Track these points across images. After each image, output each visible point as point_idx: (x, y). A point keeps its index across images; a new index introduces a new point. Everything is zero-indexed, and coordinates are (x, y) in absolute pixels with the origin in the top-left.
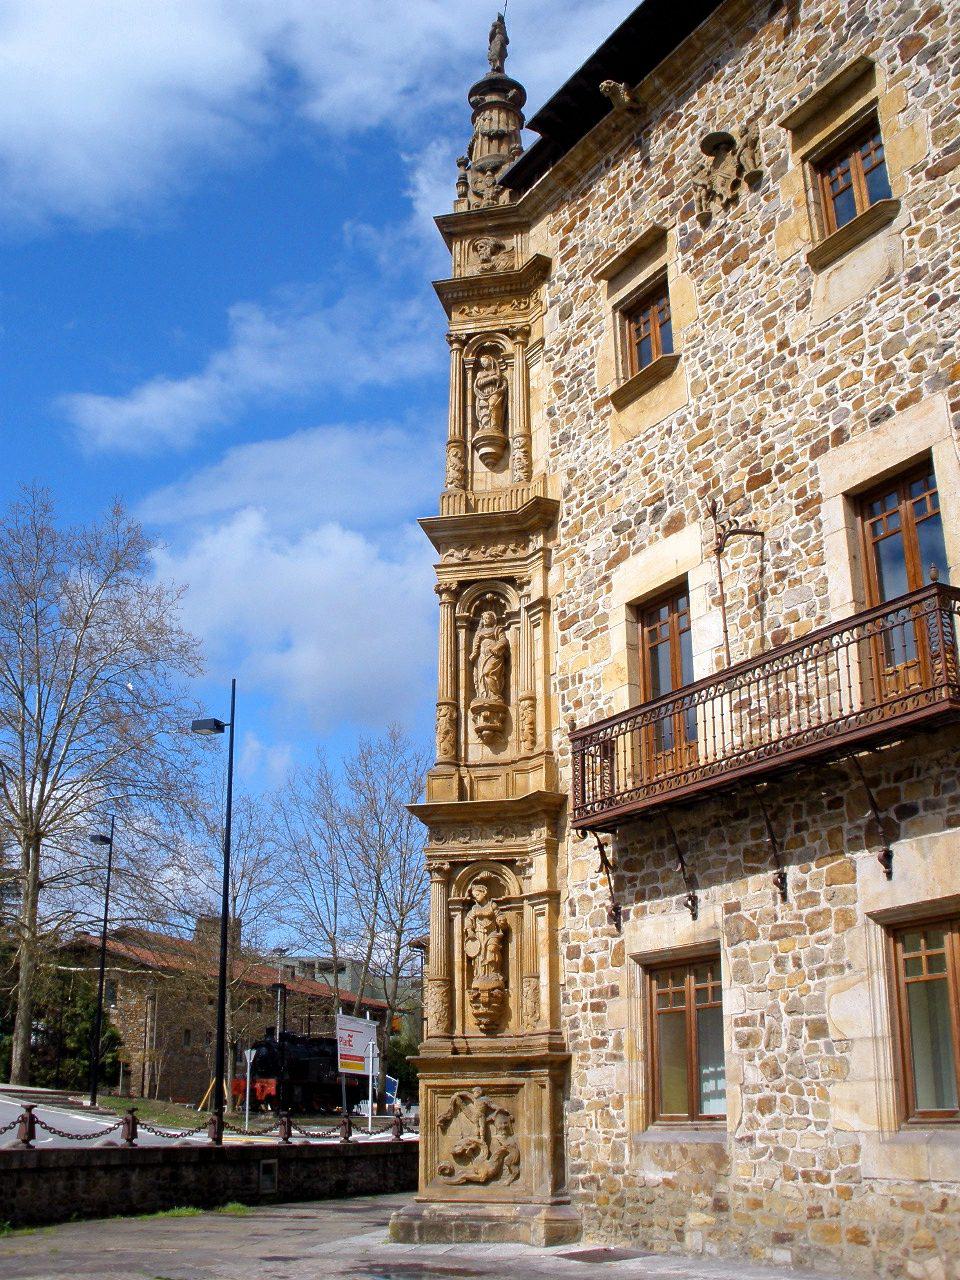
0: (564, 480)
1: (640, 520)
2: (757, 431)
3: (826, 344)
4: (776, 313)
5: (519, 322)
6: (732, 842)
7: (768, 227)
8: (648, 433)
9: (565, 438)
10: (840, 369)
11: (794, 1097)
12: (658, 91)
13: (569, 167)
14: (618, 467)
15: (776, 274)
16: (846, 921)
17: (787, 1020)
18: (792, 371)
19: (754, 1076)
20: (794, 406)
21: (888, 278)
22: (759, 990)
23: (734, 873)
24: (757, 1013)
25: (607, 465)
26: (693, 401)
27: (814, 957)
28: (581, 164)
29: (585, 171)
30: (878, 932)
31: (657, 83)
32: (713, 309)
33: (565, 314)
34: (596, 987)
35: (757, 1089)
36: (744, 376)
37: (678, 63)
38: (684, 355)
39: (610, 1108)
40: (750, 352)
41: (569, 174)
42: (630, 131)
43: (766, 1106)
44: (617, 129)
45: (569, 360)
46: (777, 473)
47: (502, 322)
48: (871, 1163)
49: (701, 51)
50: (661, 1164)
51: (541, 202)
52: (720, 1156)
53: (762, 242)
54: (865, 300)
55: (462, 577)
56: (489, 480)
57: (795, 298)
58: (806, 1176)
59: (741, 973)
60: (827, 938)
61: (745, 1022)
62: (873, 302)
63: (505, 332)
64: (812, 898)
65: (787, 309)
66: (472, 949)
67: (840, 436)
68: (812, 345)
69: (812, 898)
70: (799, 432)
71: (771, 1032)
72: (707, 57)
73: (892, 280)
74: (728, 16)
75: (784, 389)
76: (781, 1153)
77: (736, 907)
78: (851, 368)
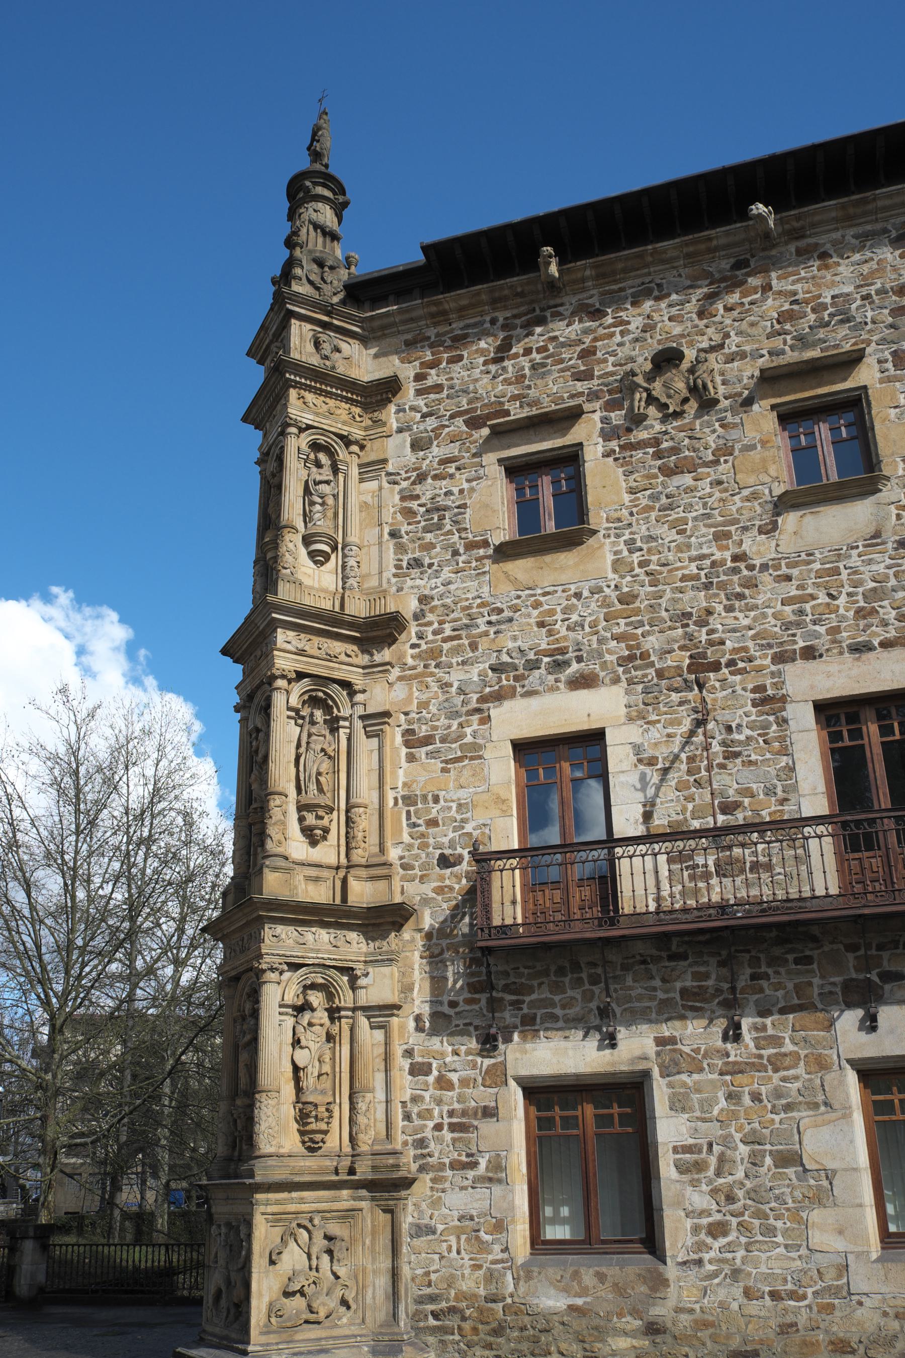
1: (533, 665)
2: (702, 623)
3: (795, 572)
4: (732, 528)
5: (357, 433)
6: (664, 980)
8: (547, 590)
9: (417, 563)
10: (813, 597)
11: (756, 1222)
12: (583, 280)
13: (447, 307)
14: (500, 611)
15: (732, 495)
16: (821, 1064)
17: (744, 1150)
18: (751, 584)
19: (699, 1199)
20: (752, 614)
21: (873, 537)
22: (704, 1120)
23: (668, 1011)
24: (704, 1142)
25: (482, 605)
26: (611, 575)
27: (778, 1094)
28: (462, 309)
29: (461, 318)
30: (852, 1077)
31: (588, 273)
32: (644, 502)
33: (417, 445)
34: (456, 1106)
35: (703, 1213)
36: (686, 572)
38: (603, 532)
39: (482, 1234)
40: (694, 553)
41: (444, 313)
42: (532, 302)
43: (718, 1230)
44: (521, 295)
45: (428, 490)
46: (728, 665)
47: (340, 426)
48: (861, 1279)
49: (647, 266)
50: (566, 1290)
51: (394, 324)
52: (659, 1283)
53: (716, 462)
54: (845, 548)
55: (300, 667)
56: (316, 578)
57: (758, 523)
58: (775, 1295)
59: (678, 1104)
60: (796, 1078)
61: (688, 1149)
62: (854, 553)
63: (341, 437)
64: (776, 1041)
65: (745, 529)
66: (302, 1058)
67: (810, 653)
68: (777, 567)
69: (776, 1041)
70: (754, 638)
71: (722, 1159)
72: (649, 274)
73: (879, 540)
74: (691, 249)
75: (740, 596)
76: (736, 1274)
77: (672, 1040)
78: (823, 599)
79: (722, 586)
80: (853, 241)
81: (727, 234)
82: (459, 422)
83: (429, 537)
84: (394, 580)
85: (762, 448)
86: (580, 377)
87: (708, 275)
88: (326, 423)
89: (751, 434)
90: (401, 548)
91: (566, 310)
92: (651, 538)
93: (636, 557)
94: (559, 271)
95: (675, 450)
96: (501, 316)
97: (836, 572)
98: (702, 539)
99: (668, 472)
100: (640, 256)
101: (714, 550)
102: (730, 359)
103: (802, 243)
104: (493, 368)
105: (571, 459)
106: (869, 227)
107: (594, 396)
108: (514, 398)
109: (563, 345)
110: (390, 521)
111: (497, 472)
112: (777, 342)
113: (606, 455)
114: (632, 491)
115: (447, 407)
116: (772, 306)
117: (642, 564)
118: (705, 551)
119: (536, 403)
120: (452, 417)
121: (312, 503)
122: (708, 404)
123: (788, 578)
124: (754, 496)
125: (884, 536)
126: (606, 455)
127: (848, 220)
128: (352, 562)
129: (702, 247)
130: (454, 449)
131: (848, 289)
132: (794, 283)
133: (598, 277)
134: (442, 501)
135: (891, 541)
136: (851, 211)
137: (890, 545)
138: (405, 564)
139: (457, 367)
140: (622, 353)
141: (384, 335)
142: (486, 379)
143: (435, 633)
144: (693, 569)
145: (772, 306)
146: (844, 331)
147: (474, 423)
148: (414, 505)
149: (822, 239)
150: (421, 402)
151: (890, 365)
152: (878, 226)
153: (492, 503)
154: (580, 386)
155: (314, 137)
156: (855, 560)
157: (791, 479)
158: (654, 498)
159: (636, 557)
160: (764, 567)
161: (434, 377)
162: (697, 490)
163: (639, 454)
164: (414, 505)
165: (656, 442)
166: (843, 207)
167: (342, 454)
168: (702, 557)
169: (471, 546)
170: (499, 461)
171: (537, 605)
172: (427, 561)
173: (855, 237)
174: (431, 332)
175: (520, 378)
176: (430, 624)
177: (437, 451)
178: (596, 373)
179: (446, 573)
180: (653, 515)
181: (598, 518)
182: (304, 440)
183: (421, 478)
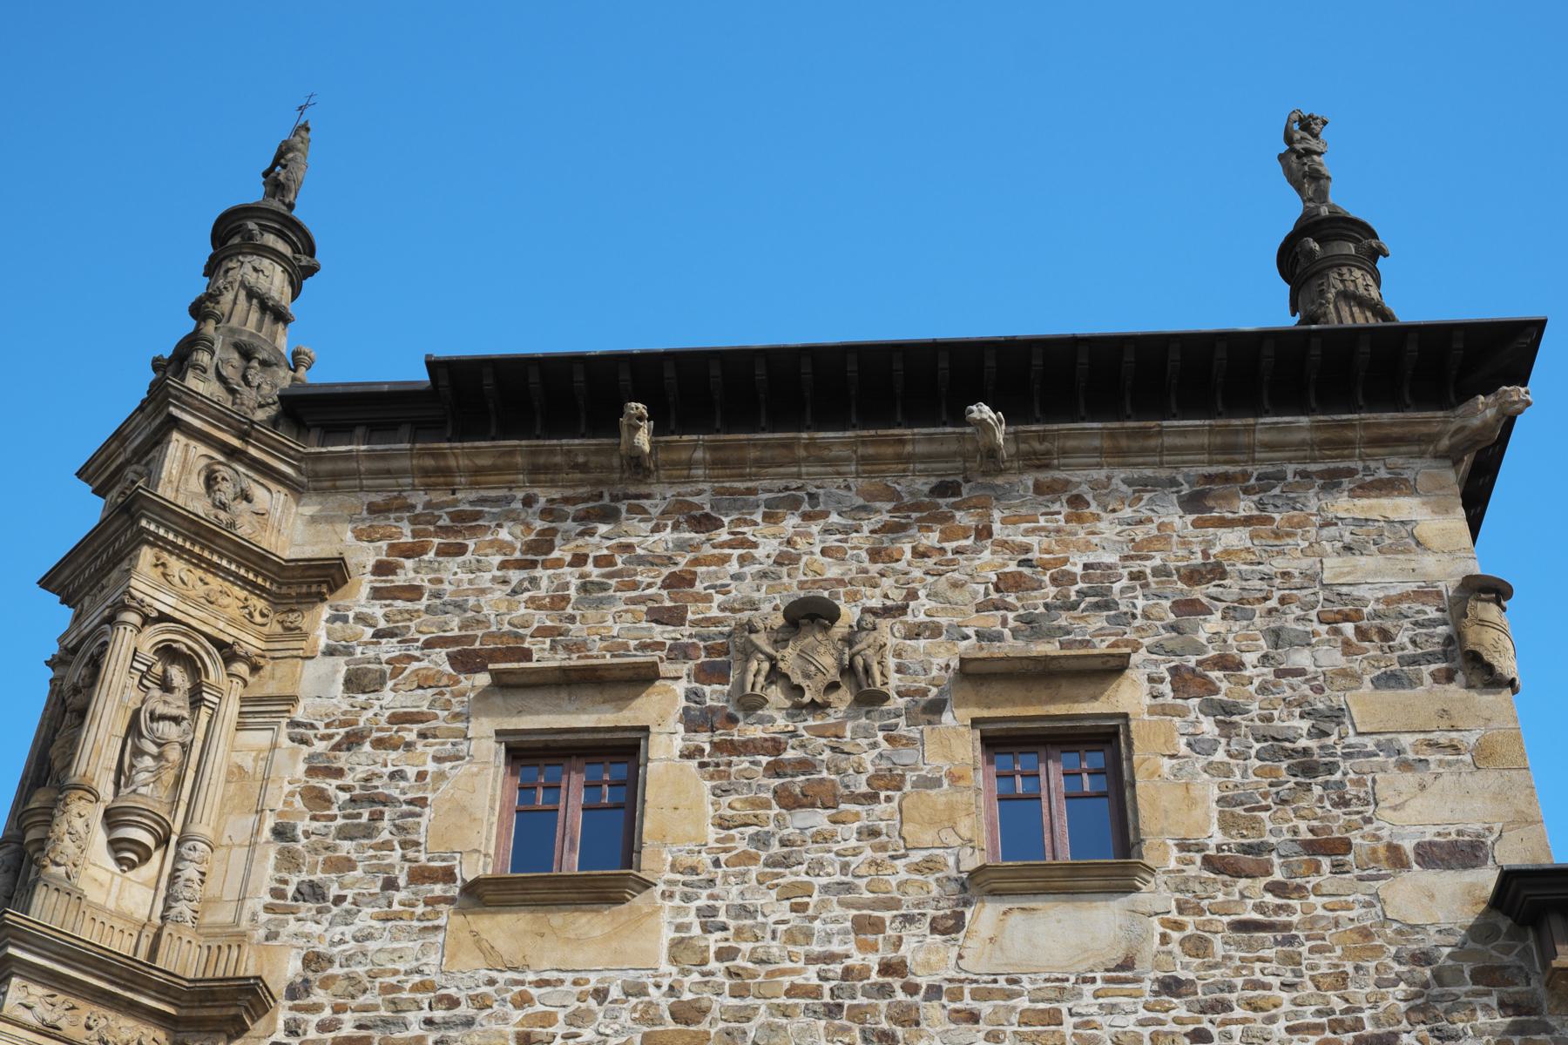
0: (292, 968)
3: (985, 1008)
4: (887, 915)
5: (251, 642)
7: (886, 781)
8: (546, 976)
9: (313, 892)
12: (690, 464)
13: (452, 463)
14: (453, 1003)
15: (893, 857)
21: (1121, 967)
25: (423, 987)
26: (665, 967)
28: (478, 471)
29: (473, 485)
31: (699, 455)
32: (742, 846)
33: (354, 683)
36: (798, 980)
37: (753, 454)
38: (661, 887)
40: (816, 948)
41: (447, 472)
42: (599, 482)
45: (360, 764)
47: (221, 625)
49: (797, 462)
51: (354, 474)
53: (872, 798)
54: (1072, 979)
56: (115, 890)
57: (931, 912)
62: (1088, 989)
63: (220, 645)
65: (908, 919)
68: (956, 996)
72: (799, 476)
73: (1129, 974)
74: (871, 451)
79: (858, 1014)
80: (1124, 488)
81: (930, 439)
82: (440, 655)
83: (346, 847)
84: (264, 917)
85: (949, 794)
86: (660, 616)
87: (894, 495)
88: (197, 617)
89: (934, 761)
90: (289, 860)
91: (654, 507)
92: (744, 911)
93: (714, 941)
94: (652, 443)
95: (806, 766)
96: (543, 496)
97: (1054, 1018)
98: (832, 927)
99: (790, 801)
100: (787, 445)
101: (851, 948)
102: (915, 633)
103: (1045, 476)
104: (515, 576)
105: (626, 750)
106: (1149, 472)
107: (680, 652)
108: (542, 632)
109: (641, 560)
110: (280, 807)
111: (490, 753)
112: (992, 621)
113: (687, 755)
114: (722, 823)
115: (422, 627)
116: (988, 562)
117: (723, 955)
118: (836, 947)
119: (578, 647)
120: (428, 644)
121: (138, 752)
122: (869, 699)
123: (973, 1018)
124: (928, 866)
125: (1139, 968)
126: (687, 755)
127: (1117, 455)
128: (190, 871)
129: (889, 451)
130: (421, 701)
131: (1110, 558)
132: (1027, 533)
133: (715, 464)
134: (383, 787)
135: (1150, 977)
136: (1124, 443)
137: (1147, 986)
138: (291, 890)
139: (453, 564)
140: (738, 591)
141: (335, 488)
142: (500, 593)
143: (323, 1027)
144: (811, 976)
145: (988, 562)
146: (1098, 621)
147: (466, 662)
148: (330, 785)
149: (1076, 476)
150: (377, 610)
151: (1166, 688)
152: (1164, 473)
153: (471, 809)
154: (660, 633)
155: (280, 158)
156: (1087, 1003)
157: (994, 848)
158: (761, 841)
159: (714, 941)
160: (934, 992)
161: (408, 573)
162: (832, 841)
163: (742, 763)
164: (330, 785)
165: (776, 747)
166: (1112, 434)
167: (215, 672)
168: (830, 958)
169: (420, 876)
170: (498, 733)
171: (523, 1001)
172: (334, 891)
173: (1128, 482)
174: (419, 499)
175: (558, 601)
176: (316, 1008)
177: (390, 699)
178: (690, 616)
179: (365, 919)
180: (755, 870)
181: (656, 860)
182: (151, 638)
183: (352, 741)
